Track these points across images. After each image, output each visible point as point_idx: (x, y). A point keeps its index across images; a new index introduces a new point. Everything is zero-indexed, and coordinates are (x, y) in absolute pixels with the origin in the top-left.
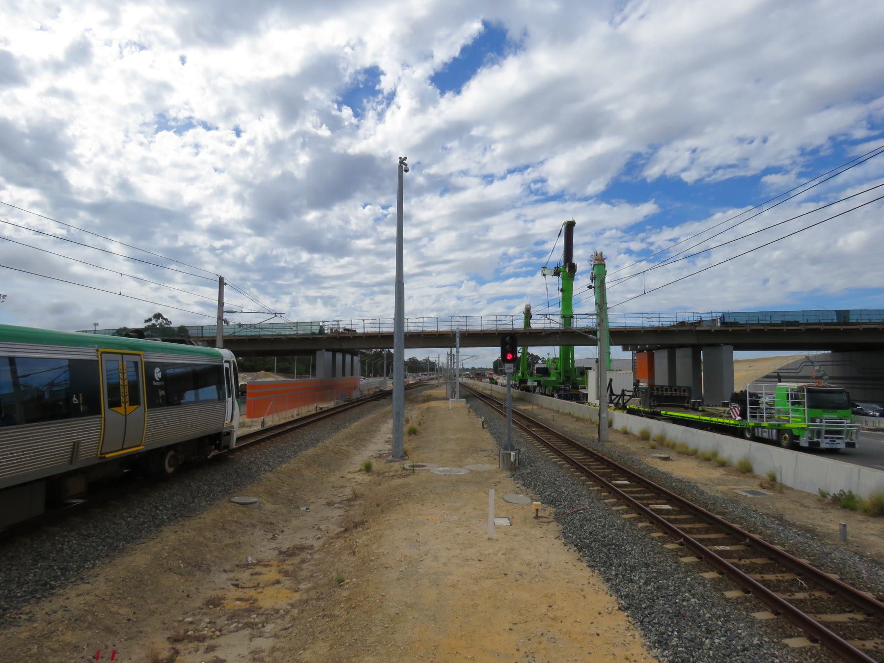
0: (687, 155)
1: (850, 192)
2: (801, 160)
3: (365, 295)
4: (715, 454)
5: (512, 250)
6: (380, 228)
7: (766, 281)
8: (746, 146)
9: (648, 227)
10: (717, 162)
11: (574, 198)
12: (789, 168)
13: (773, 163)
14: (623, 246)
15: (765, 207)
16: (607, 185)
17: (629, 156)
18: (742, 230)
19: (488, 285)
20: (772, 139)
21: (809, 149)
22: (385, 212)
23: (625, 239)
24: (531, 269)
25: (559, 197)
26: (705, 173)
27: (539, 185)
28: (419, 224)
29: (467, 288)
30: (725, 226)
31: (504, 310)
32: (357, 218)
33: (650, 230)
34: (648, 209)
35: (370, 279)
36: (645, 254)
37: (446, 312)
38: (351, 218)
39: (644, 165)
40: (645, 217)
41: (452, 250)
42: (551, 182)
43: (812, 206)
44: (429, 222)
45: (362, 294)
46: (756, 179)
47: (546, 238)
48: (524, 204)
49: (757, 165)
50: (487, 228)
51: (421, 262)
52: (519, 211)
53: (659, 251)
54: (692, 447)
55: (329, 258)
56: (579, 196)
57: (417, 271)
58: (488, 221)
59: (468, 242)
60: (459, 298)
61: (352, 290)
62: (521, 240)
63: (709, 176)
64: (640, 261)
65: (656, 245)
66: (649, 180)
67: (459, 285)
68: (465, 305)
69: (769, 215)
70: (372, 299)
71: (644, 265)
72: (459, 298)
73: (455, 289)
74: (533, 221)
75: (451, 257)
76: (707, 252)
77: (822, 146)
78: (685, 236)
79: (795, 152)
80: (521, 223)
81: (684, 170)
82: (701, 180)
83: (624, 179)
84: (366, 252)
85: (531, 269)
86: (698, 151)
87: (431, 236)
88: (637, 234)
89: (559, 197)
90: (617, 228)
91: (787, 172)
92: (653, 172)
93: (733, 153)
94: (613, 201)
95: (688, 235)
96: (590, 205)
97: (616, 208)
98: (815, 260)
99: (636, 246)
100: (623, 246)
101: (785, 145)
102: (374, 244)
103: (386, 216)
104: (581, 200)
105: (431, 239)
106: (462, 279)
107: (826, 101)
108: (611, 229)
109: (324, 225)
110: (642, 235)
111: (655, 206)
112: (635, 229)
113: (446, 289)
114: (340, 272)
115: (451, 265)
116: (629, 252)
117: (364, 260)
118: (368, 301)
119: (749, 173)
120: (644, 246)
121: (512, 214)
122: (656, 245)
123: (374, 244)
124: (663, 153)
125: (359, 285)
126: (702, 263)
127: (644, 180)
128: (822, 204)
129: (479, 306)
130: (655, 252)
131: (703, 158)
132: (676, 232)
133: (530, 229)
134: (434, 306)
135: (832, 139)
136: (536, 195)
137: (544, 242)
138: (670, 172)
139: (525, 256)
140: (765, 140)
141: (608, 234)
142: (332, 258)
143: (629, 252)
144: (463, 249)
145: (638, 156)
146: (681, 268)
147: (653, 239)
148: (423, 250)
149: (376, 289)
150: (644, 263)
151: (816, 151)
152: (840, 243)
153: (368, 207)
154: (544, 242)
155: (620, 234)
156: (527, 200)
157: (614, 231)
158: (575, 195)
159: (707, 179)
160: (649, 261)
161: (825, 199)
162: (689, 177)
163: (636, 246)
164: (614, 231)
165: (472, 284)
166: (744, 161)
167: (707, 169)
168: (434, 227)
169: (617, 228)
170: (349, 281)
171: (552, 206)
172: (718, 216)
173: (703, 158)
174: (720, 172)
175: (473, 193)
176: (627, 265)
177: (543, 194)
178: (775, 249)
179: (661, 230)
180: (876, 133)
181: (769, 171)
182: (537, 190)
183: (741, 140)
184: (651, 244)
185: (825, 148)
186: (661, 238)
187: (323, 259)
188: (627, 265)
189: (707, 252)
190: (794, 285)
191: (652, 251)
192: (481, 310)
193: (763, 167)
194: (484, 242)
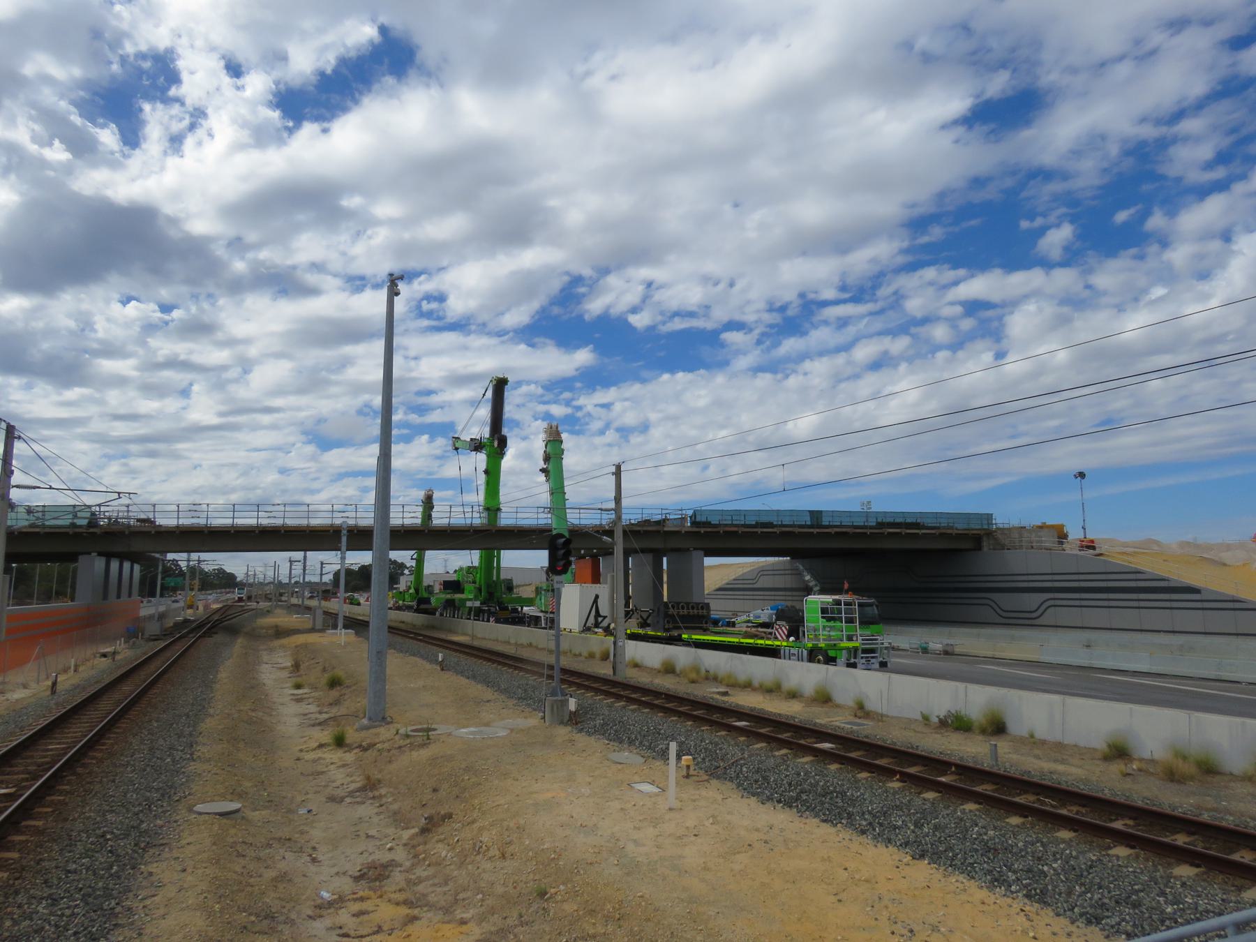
3: (110, 458)
6: (153, 342)
11: (483, 329)
19: (335, 451)
22: (166, 317)
24: (405, 431)
28: (231, 342)
29: (301, 456)
31: (357, 493)
32: (109, 320)
35: (121, 429)
37: (259, 492)
38: (96, 318)
41: (279, 391)
44: (247, 341)
45: (105, 456)
47: (433, 386)
50: (345, 363)
51: (223, 408)
55: (42, 387)
57: (216, 421)
58: (349, 349)
59: (312, 382)
60: (283, 471)
61: (85, 446)
67: (283, 449)
68: (293, 482)
70: (125, 465)
72: (283, 471)
73: (280, 454)
75: (278, 402)
84: (120, 381)
85: (405, 431)
87: (246, 366)
89: (461, 326)
100: (542, 408)
102: (137, 369)
103: (167, 323)
104: (489, 334)
105: (246, 371)
106: (292, 439)
109: (39, 325)
113: (263, 455)
114: (64, 413)
115: (276, 416)
117: (114, 398)
118: (114, 467)
123: (137, 369)
125: (101, 439)
129: (316, 485)
133: (411, 370)
134: (238, 482)
138: (615, 312)
142: (49, 388)
144: (301, 391)
147: (582, 401)
148: (232, 388)
149: (134, 448)
153: (133, 303)
154: (429, 393)
157: (533, 387)
165: (310, 449)
168: (253, 351)
170: (79, 430)
175: (331, 303)
179: (594, 390)
187: (29, 387)
191: (578, 419)
192: (319, 491)
194: (337, 383)
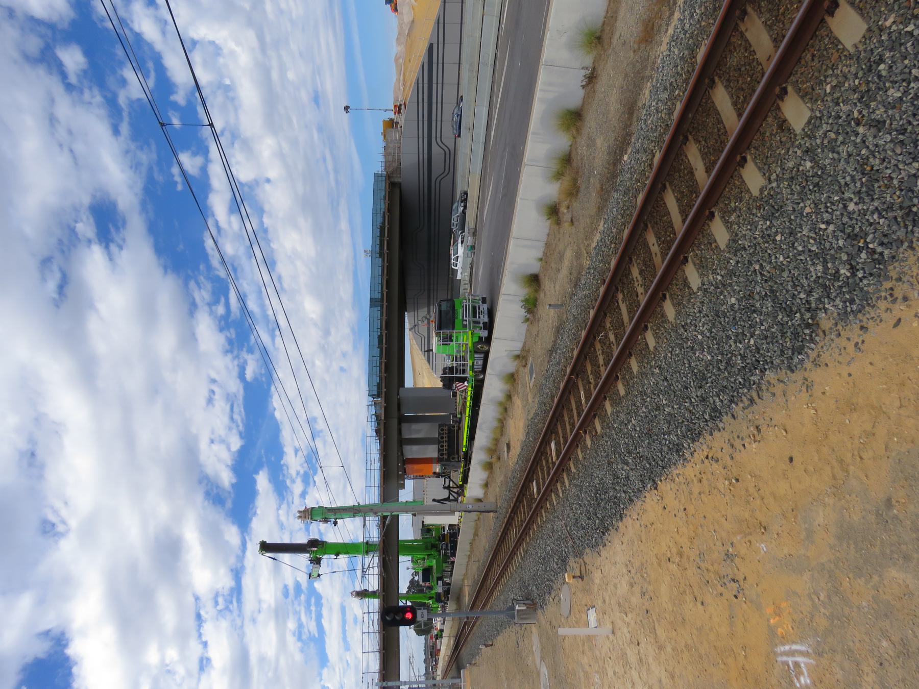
0: (215, 447)
1: (270, 313)
2: (235, 352)
4: (501, 404)
5: (291, 625)
7: (342, 369)
8: (217, 397)
9: (281, 478)
10: (226, 420)
12: (242, 361)
13: (235, 372)
14: (297, 500)
15: (275, 376)
16: (233, 523)
17: (206, 503)
18: (292, 392)
20: (214, 375)
21: (228, 347)
23: (290, 500)
25: (237, 574)
26: (234, 431)
27: (220, 600)
30: (289, 408)
33: (284, 475)
34: (262, 481)
36: (307, 479)
39: (218, 487)
40: (270, 481)
42: (219, 586)
43: (278, 340)
46: (248, 387)
48: (239, 616)
49: (235, 386)
52: (247, 621)
53: (306, 465)
54: (496, 424)
56: (239, 553)
62: (279, 614)
63: (238, 426)
64: (315, 482)
65: (299, 468)
66: (234, 481)
69: (282, 372)
71: (318, 478)
74: (260, 602)
76: (311, 422)
77: (227, 337)
78: (293, 443)
79: (230, 356)
80: (261, 618)
81: (229, 449)
82: (240, 434)
83: (229, 504)
86: (213, 437)
88: (286, 488)
90: (278, 509)
91: (245, 362)
92: (226, 478)
93: (221, 405)
94: (250, 516)
95: (292, 439)
96: (251, 540)
97: (258, 512)
98: (327, 333)
99: (298, 488)
101: (221, 366)
107: (189, 339)
108: (278, 516)
110: (288, 482)
111: (261, 473)
112: (281, 488)
116: (303, 495)
119: (242, 392)
120: (299, 481)
121: (249, 629)
122: (299, 468)
124: (210, 471)
126: (321, 425)
127: (233, 486)
128: (277, 333)
130: (306, 469)
131: (222, 432)
132: (289, 450)
135: (221, 330)
136: (231, 602)
137: (286, 587)
139: (298, 609)
140: (214, 381)
141: (283, 519)
143: (303, 495)
145: (208, 494)
146: (325, 442)
150: (316, 478)
151: (230, 341)
152: (314, 316)
155: (284, 506)
156: (236, 613)
158: (238, 557)
159: (241, 428)
160: (315, 473)
161: (273, 330)
162: (236, 443)
163: (298, 488)
164: (281, 512)
166: (230, 399)
167: (230, 429)
169: (278, 509)
171: (247, 581)
172: (277, 415)
173: (222, 432)
174: (236, 417)
176: (317, 495)
177: (231, 595)
178: (313, 365)
180: (223, 300)
181: (242, 376)
182: (225, 600)
183: (210, 401)
184: (298, 473)
185: (229, 335)
186: (293, 463)
188: (317, 495)
189: (311, 422)
190: (347, 347)
193: (238, 381)
